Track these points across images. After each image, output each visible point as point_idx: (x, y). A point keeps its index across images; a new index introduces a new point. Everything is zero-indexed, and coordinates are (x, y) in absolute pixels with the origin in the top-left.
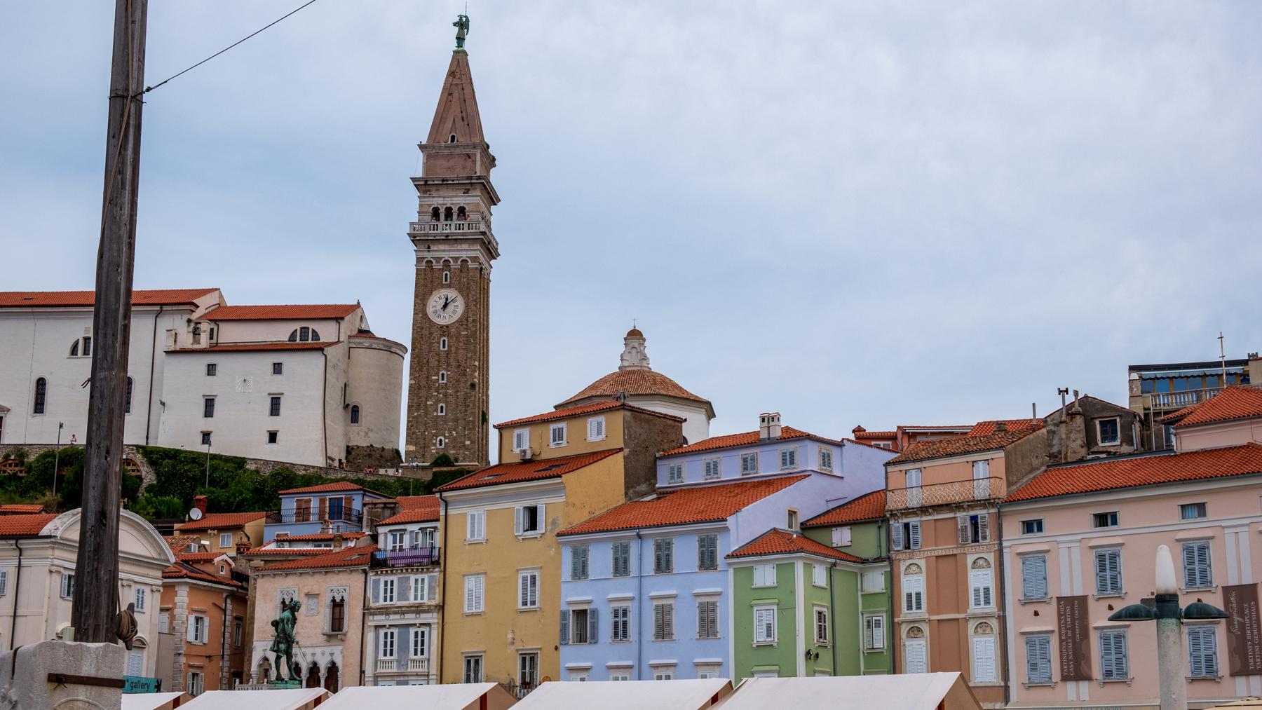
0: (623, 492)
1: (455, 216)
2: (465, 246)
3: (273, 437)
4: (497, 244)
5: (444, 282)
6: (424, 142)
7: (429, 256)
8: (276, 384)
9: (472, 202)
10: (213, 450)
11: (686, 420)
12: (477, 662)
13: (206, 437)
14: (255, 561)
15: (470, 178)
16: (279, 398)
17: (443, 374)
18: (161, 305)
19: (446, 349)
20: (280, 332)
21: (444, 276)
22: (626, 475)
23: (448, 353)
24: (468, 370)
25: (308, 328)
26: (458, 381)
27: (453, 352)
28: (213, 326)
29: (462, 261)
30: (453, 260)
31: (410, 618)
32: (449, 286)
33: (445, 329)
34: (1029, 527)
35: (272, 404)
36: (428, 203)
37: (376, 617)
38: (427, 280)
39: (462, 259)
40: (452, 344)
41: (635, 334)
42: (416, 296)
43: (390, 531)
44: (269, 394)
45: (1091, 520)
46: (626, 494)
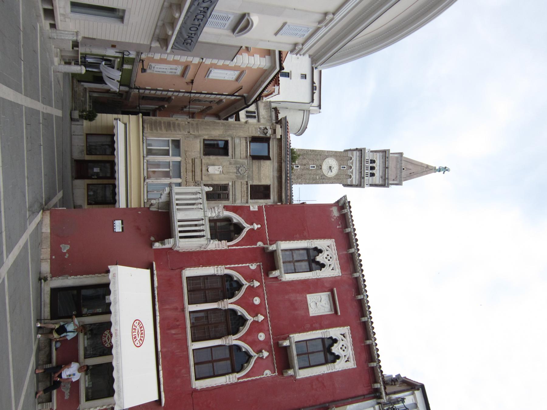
1: (371, 171)
5: (341, 166)
6: (404, 156)
7: (354, 158)
9: (377, 180)
14: (280, 129)
16: (289, 77)
17: (298, 167)
19: (311, 168)
21: (344, 166)
23: (308, 169)
24: (300, 180)
27: (309, 172)
29: (351, 176)
30: (351, 171)
32: (340, 169)
33: (320, 167)
36: (377, 158)
39: (352, 175)
40: (313, 171)
42: (336, 152)
44: (291, 71)
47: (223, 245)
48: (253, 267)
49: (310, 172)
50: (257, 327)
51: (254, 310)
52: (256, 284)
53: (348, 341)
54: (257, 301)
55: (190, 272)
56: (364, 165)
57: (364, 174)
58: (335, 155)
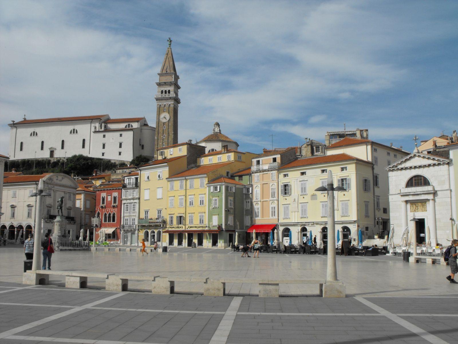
0: (187, 167)
1: (167, 93)
2: (170, 101)
3: (120, 154)
4: (180, 100)
6: (159, 73)
7: (160, 104)
8: (121, 140)
10: (106, 157)
11: (206, 147)
12: (147, 212)
13: (103, 154)
15: (171, 82)
18: (92, 119)
20: (123, 126)
22: (188, 162)
25: (130, 124)
26: (168, 138)
28: (106, 124)
31: (132, 201)
32: (166, 111)
34: (285, 176)
35: (120, 145)
37: (124, 201)
38: (160, 111)
41: (218, 124)
42: (157, 114)
43: (128, 178)
45: (300, 174)
46: (187, 167)
47: (100, 215)
48: (103, 210)
49: (167, 129)
50: (111, 211)
51: (109, 211)
52: (105, 210)
53: (114, 193)
54: (108, 210)
55: (103, 222)
56: (164, 98)
57: (168, 97)
58: (159, 114)
